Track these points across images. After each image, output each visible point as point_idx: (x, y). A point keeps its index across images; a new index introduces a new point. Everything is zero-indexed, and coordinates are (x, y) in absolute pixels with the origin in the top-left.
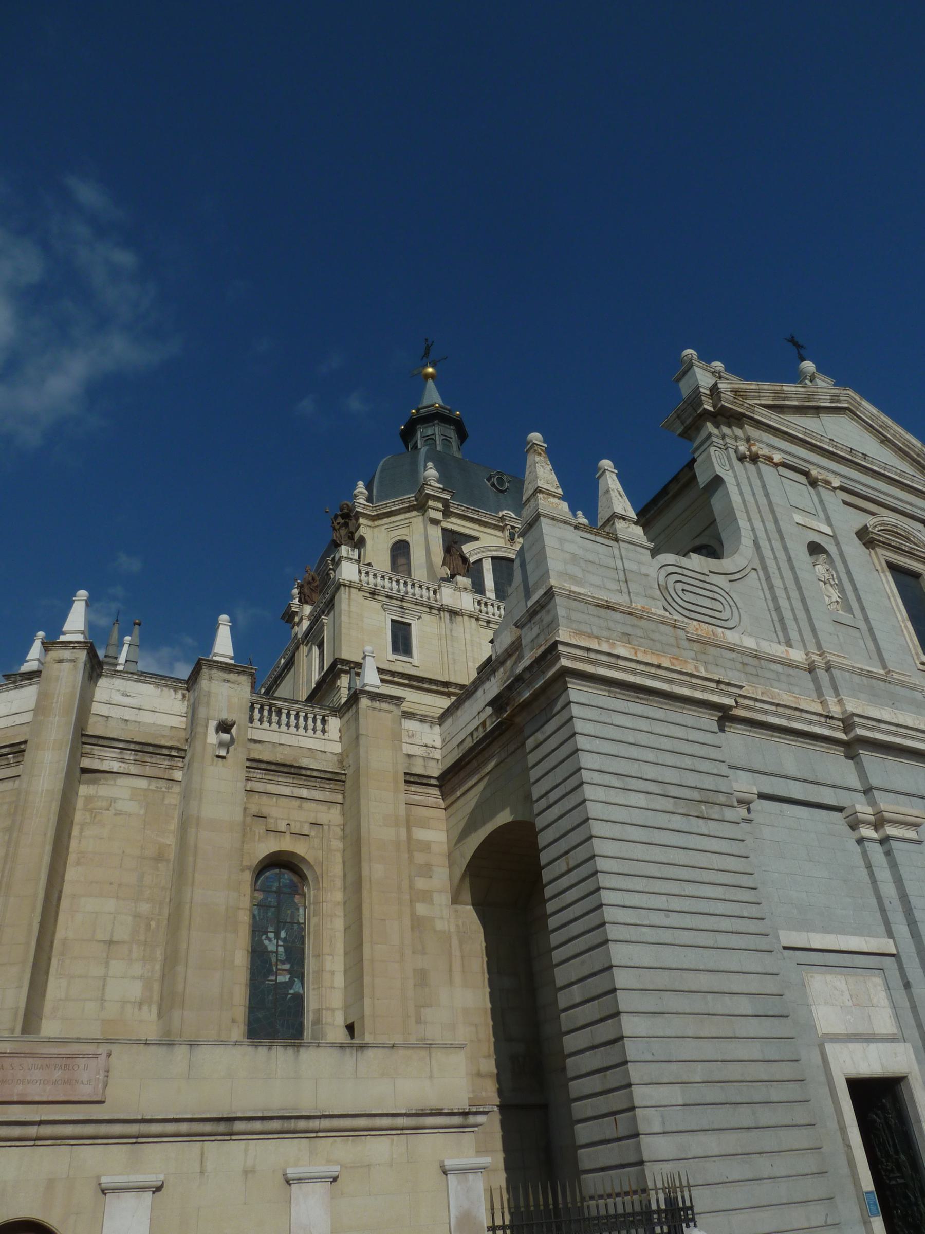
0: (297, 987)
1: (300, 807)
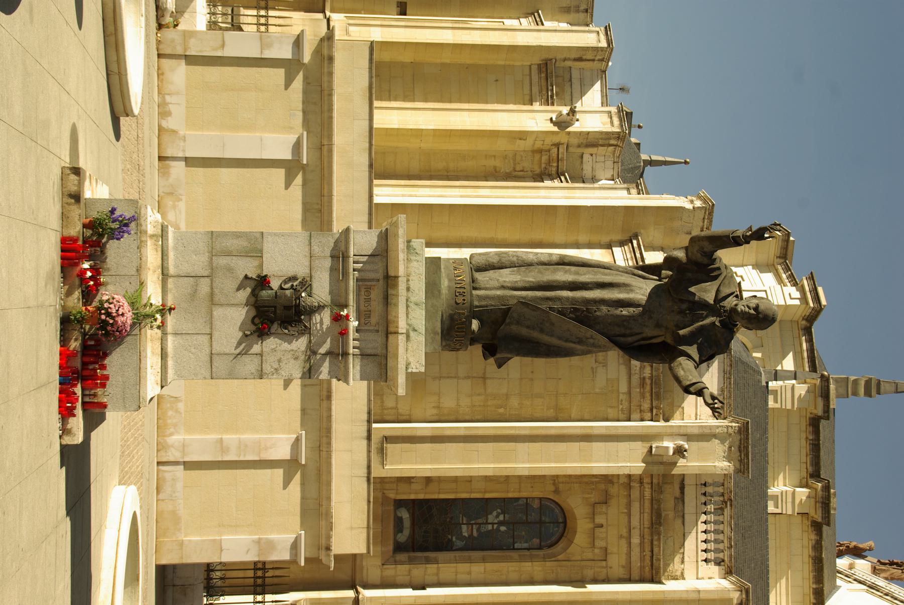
0: (459, 544)
1: (621, 537)
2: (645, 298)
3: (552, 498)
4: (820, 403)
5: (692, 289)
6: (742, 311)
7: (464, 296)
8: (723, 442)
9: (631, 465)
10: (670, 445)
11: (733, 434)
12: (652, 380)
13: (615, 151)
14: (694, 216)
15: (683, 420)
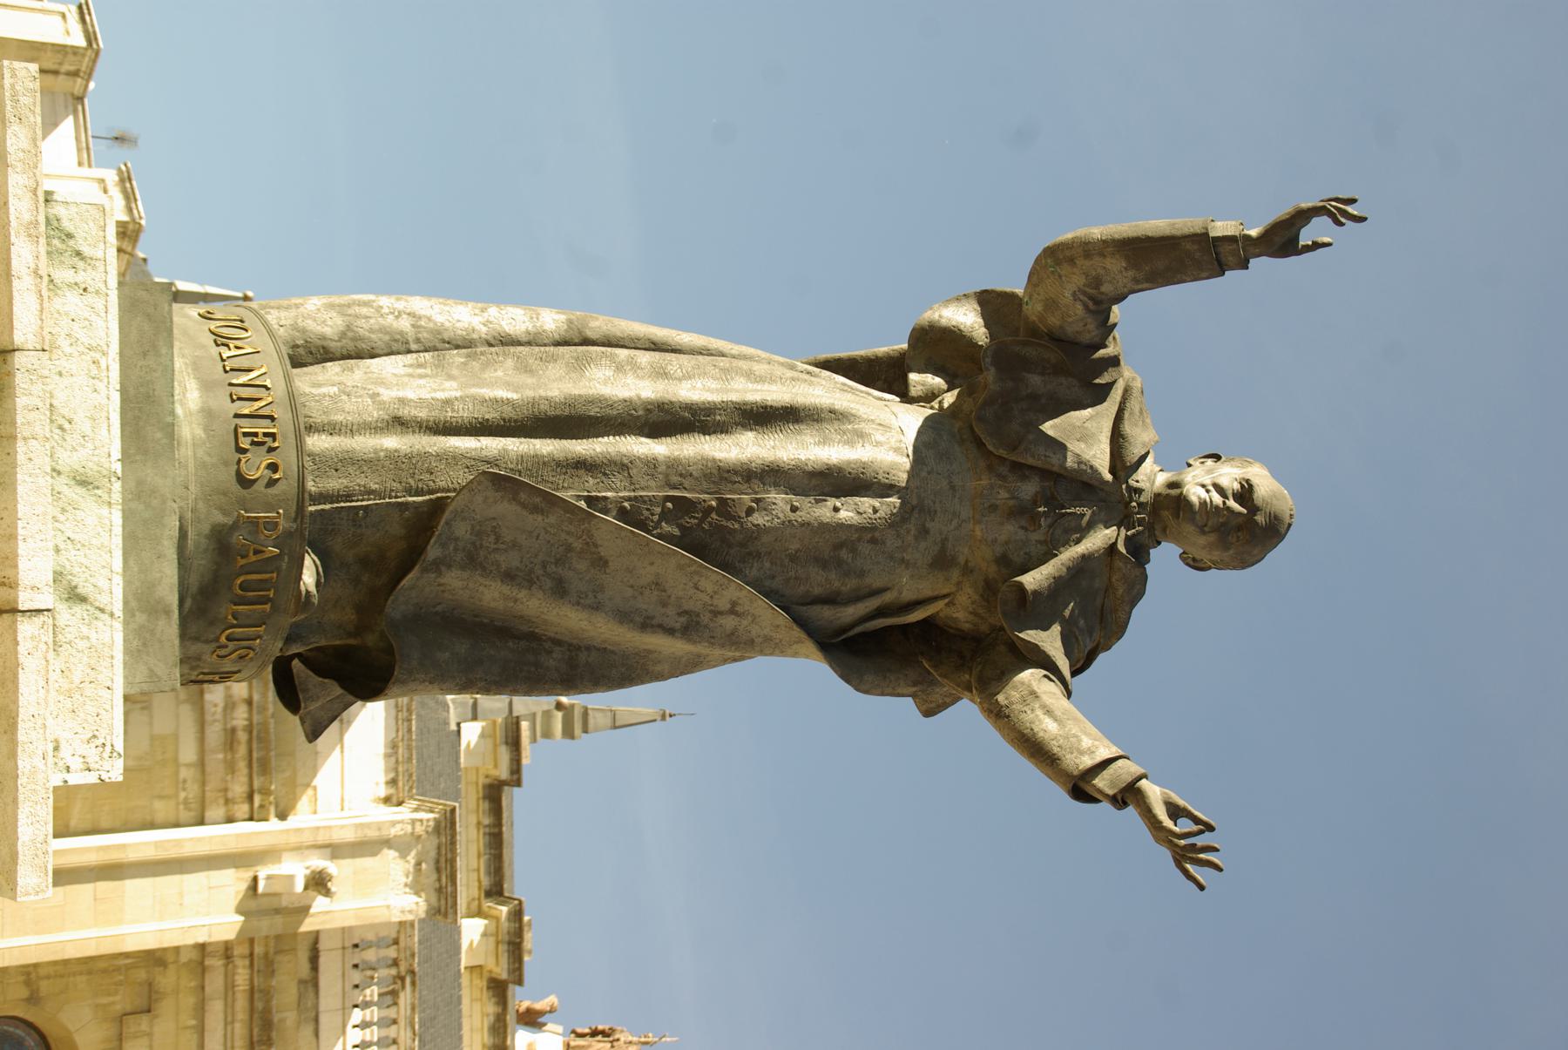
2: (906, 463)
3: (21, 1015)
4: (504, 755)
5: (1049, 427)
7: (271, 450)
8: (403, 855)
10: (296, 869)
11: (424, 836)
12: (250, 732)
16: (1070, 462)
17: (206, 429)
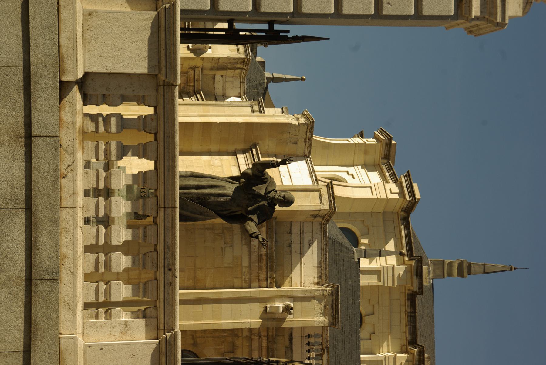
2: (232, 193)
4: (415, 281)
5: (254, 188)
6: (277, 198)
8: (320, 302)
9: (251, 321)
12: (267, 256)
13: (241, 73)
14: (299, 130)
15: (291, 287)
16: (256, 193)
17: (138, 190)
